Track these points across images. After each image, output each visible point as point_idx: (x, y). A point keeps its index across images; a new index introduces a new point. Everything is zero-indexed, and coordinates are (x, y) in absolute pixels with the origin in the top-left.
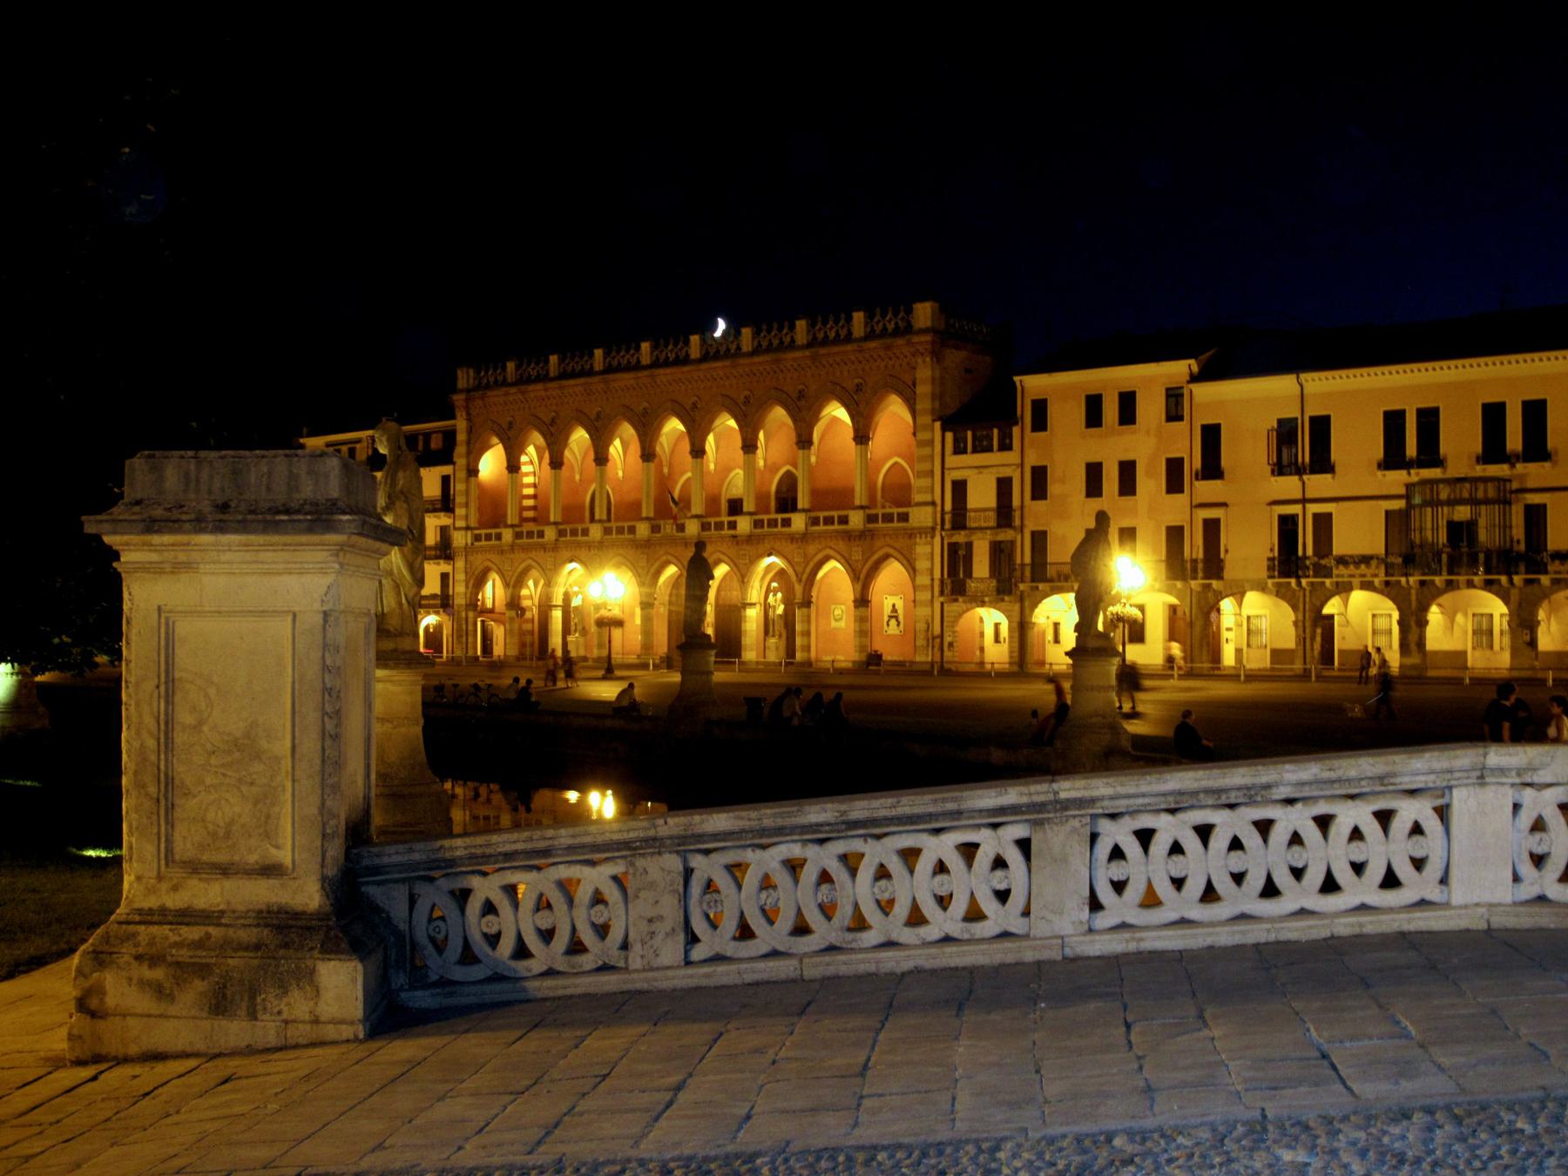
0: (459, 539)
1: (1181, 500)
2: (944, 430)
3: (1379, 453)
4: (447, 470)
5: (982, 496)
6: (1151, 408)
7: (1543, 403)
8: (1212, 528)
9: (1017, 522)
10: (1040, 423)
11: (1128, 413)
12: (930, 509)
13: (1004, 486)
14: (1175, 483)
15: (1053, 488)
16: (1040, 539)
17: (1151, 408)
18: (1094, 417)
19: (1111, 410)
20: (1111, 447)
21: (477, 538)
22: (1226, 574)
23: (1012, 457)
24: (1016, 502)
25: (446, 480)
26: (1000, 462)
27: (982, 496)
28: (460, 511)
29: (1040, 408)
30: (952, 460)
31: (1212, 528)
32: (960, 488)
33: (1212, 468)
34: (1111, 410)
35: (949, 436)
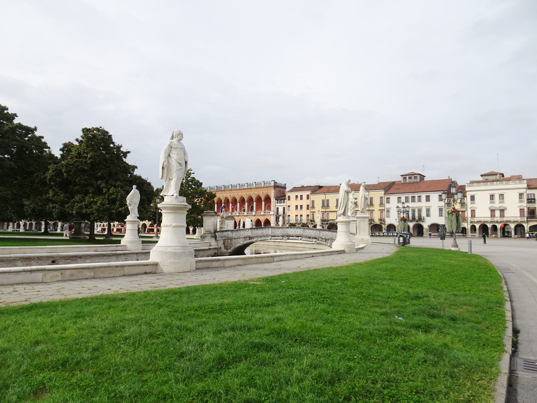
1: (309, 211)
5: (281, 211)
6: (305, 197)
10: (289, 199)
11: (301, 198)
13: (284, 208)
14: (308, 209)
17: (305, 197)
19: (299, 197)
20: (299, 203)
23: (285, 204)
27: (281, 211)
29: (289, 197)
30: (277, 205)
32: (278, 208)
33: (313, 207)
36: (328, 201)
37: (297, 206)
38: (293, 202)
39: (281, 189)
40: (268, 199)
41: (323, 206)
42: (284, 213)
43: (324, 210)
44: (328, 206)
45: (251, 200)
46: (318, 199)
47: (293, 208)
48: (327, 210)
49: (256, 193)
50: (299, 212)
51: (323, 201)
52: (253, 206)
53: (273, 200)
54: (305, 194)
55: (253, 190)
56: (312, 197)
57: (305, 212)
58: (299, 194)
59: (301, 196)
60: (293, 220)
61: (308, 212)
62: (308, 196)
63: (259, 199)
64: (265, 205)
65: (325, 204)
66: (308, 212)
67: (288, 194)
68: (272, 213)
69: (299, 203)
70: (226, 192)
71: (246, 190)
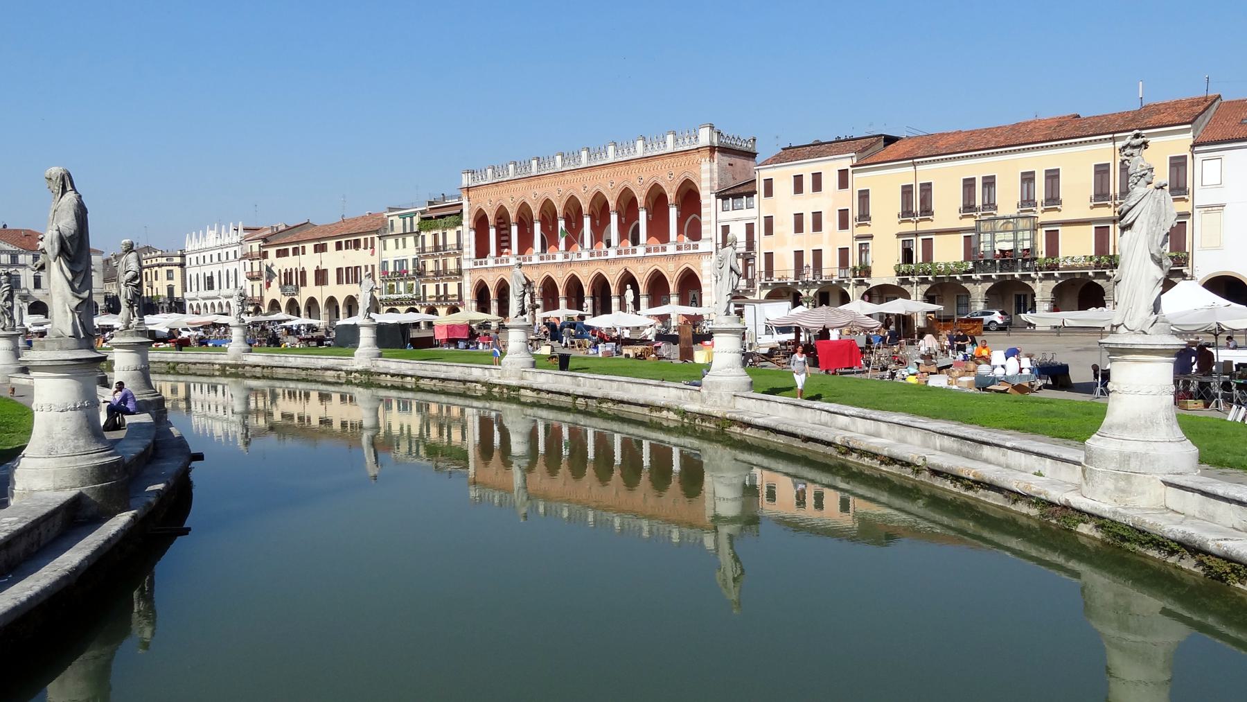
0: (466, 265)
1: (847, 234)
2: (717, 197)
3: (899, 209)
4: (459, 228)
5: (738, 232)
6: (830, 181)
7: (930, 184)
8: (863, 249)
9: (757, 248)
10: (769, 192)
12: (709, 243)
13: (750, 228)
14: (843, 224)
15: (776, 228)
16: (769, 257)
17: (830, 181)
18: (798, 188)
19: (808, 183)
20: (808, 203)
21: (476, 264)
22: (872, 275)
24: (756, 238)
25: (459, 233)
26: (748, 214)
28: (466, 250)
29: (769, 183)
31: (863, 249)
32: (726, 229)
33: (864, 216)
34: (808, 183)
35: (720, 201)
36: (926, 188)
37: (799, 218)
38: (784, 204)
39: (739, 162)
40: (689, 198)
41: (907, 213)
42: (750, 244)
43: (909, 227)
44: (927, 211)
45: (628, 205)
46: (885, 184)
47: (784, 225)
48: (923, 226)
49: (645, 177)
50: (808, 242)
51: (907, 191)
52: (637, 228)
53: (708, 201)
54: (830, 168)
55: (634, 166)
56: (859, 181)
57: (831, 240)
58: (806, 169)
59: (817, 178)
60: (785, 269)
61: (846, 239)
62: (843, 174)
63: (657, 200)
64: (681, 221)
65: (917, 203)
66: (846, 239)
67: (763, 174)
68: (703, 246)
69: (808, 203)
70: (544, 180)
71: (611, 170)
